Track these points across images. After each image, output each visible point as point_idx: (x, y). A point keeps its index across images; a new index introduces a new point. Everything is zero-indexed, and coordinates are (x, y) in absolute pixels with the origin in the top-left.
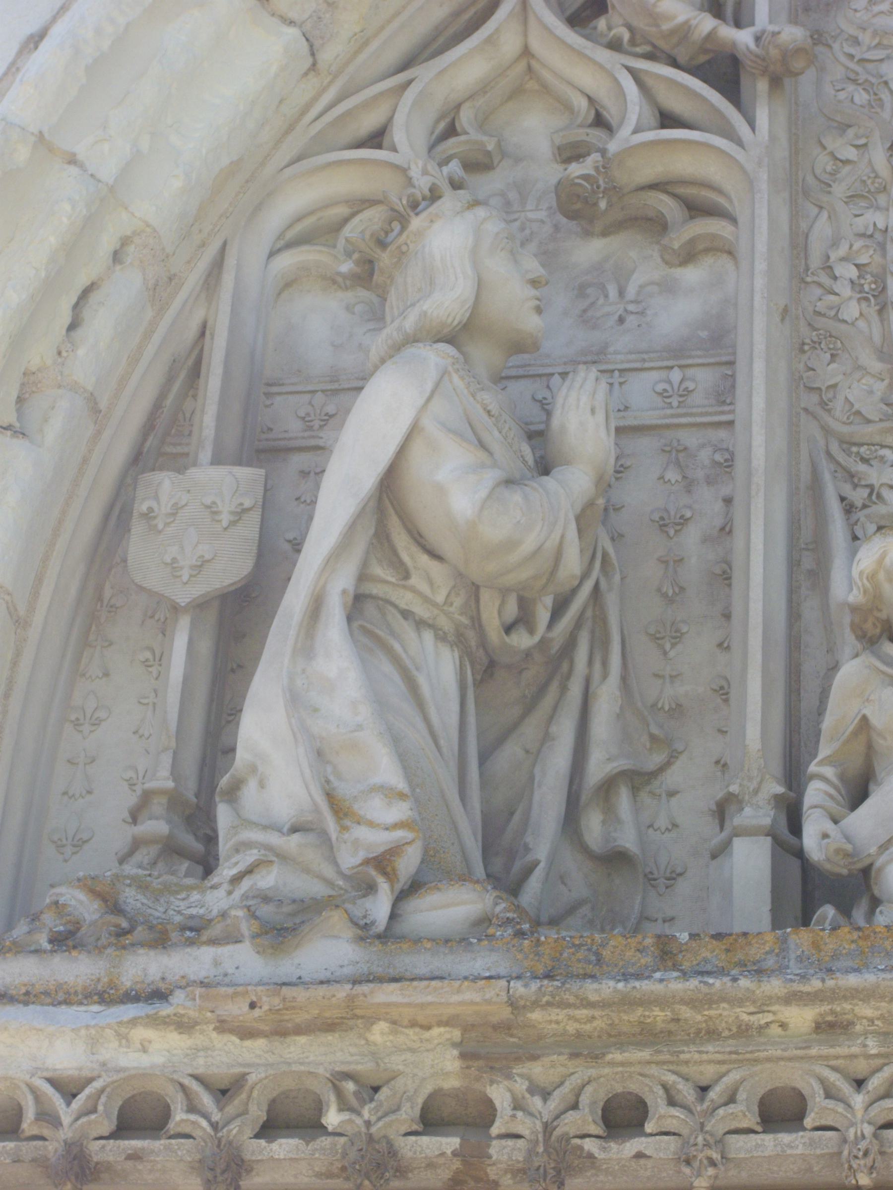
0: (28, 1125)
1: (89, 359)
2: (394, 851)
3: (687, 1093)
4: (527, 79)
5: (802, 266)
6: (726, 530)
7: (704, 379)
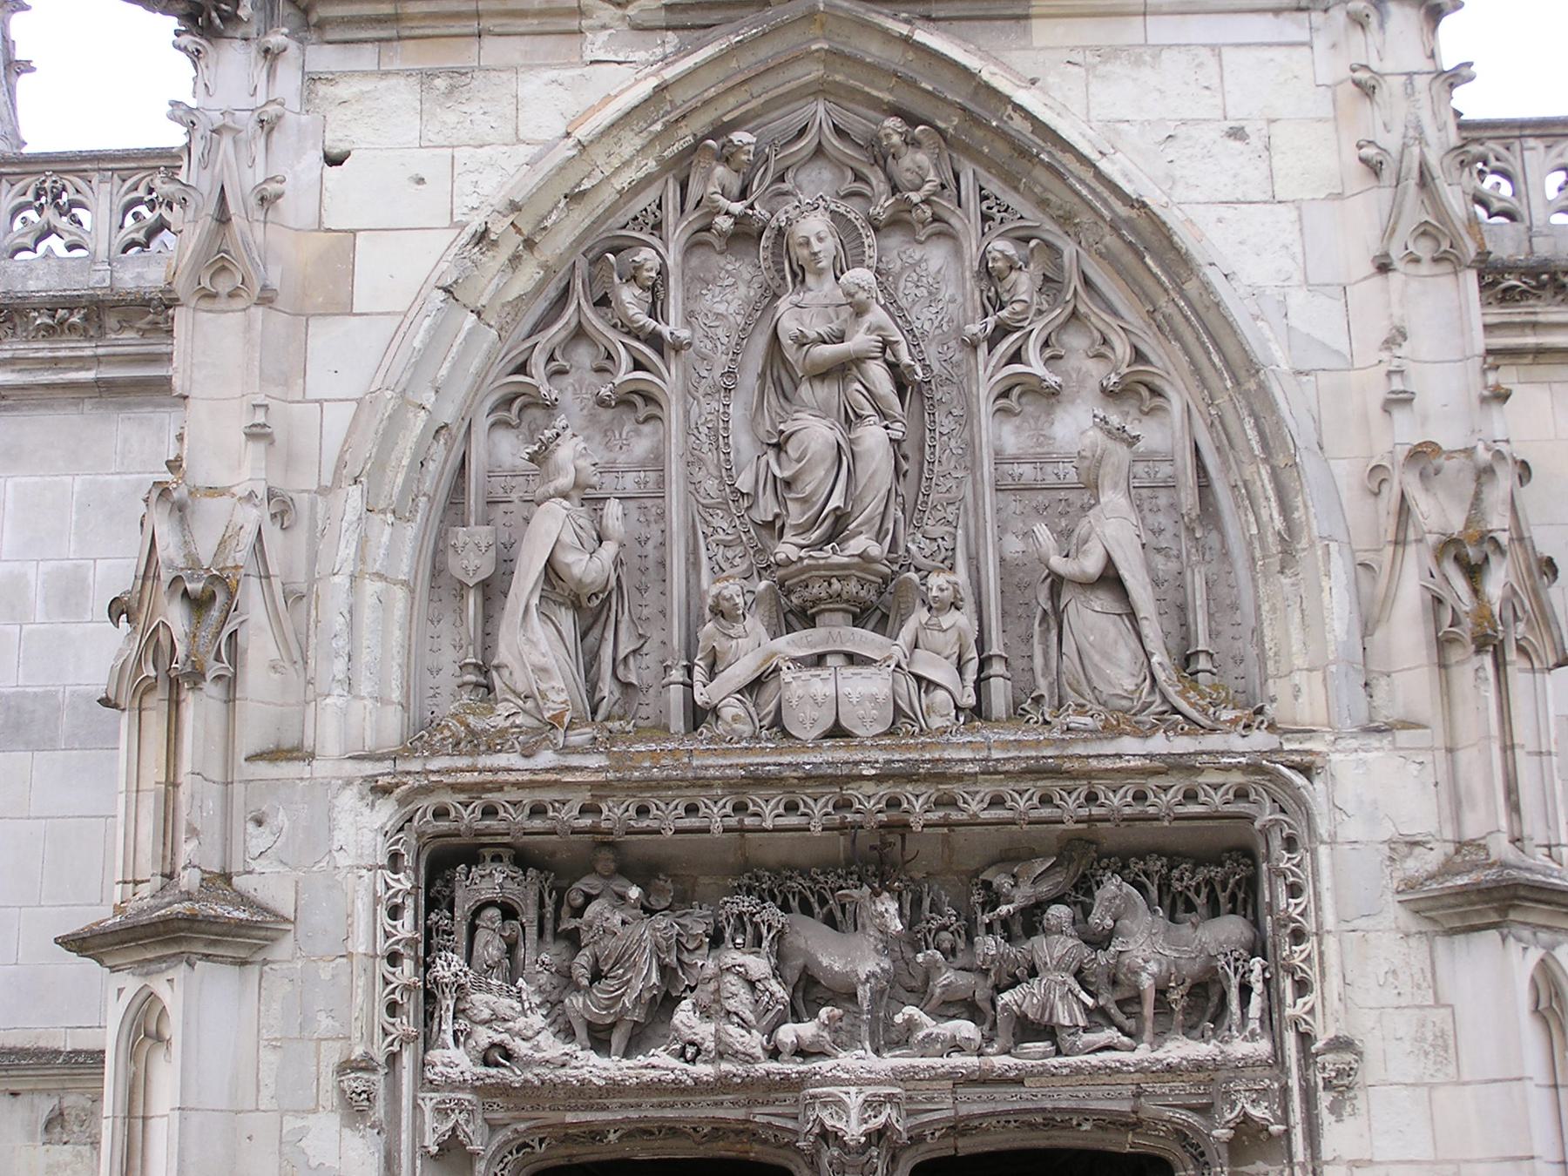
0: (453, 813)
1: (427, 486)
3: (662, 806)
4: (580, 333)
5: (689, 431)
6: (663, 544)
7: (652, 476)
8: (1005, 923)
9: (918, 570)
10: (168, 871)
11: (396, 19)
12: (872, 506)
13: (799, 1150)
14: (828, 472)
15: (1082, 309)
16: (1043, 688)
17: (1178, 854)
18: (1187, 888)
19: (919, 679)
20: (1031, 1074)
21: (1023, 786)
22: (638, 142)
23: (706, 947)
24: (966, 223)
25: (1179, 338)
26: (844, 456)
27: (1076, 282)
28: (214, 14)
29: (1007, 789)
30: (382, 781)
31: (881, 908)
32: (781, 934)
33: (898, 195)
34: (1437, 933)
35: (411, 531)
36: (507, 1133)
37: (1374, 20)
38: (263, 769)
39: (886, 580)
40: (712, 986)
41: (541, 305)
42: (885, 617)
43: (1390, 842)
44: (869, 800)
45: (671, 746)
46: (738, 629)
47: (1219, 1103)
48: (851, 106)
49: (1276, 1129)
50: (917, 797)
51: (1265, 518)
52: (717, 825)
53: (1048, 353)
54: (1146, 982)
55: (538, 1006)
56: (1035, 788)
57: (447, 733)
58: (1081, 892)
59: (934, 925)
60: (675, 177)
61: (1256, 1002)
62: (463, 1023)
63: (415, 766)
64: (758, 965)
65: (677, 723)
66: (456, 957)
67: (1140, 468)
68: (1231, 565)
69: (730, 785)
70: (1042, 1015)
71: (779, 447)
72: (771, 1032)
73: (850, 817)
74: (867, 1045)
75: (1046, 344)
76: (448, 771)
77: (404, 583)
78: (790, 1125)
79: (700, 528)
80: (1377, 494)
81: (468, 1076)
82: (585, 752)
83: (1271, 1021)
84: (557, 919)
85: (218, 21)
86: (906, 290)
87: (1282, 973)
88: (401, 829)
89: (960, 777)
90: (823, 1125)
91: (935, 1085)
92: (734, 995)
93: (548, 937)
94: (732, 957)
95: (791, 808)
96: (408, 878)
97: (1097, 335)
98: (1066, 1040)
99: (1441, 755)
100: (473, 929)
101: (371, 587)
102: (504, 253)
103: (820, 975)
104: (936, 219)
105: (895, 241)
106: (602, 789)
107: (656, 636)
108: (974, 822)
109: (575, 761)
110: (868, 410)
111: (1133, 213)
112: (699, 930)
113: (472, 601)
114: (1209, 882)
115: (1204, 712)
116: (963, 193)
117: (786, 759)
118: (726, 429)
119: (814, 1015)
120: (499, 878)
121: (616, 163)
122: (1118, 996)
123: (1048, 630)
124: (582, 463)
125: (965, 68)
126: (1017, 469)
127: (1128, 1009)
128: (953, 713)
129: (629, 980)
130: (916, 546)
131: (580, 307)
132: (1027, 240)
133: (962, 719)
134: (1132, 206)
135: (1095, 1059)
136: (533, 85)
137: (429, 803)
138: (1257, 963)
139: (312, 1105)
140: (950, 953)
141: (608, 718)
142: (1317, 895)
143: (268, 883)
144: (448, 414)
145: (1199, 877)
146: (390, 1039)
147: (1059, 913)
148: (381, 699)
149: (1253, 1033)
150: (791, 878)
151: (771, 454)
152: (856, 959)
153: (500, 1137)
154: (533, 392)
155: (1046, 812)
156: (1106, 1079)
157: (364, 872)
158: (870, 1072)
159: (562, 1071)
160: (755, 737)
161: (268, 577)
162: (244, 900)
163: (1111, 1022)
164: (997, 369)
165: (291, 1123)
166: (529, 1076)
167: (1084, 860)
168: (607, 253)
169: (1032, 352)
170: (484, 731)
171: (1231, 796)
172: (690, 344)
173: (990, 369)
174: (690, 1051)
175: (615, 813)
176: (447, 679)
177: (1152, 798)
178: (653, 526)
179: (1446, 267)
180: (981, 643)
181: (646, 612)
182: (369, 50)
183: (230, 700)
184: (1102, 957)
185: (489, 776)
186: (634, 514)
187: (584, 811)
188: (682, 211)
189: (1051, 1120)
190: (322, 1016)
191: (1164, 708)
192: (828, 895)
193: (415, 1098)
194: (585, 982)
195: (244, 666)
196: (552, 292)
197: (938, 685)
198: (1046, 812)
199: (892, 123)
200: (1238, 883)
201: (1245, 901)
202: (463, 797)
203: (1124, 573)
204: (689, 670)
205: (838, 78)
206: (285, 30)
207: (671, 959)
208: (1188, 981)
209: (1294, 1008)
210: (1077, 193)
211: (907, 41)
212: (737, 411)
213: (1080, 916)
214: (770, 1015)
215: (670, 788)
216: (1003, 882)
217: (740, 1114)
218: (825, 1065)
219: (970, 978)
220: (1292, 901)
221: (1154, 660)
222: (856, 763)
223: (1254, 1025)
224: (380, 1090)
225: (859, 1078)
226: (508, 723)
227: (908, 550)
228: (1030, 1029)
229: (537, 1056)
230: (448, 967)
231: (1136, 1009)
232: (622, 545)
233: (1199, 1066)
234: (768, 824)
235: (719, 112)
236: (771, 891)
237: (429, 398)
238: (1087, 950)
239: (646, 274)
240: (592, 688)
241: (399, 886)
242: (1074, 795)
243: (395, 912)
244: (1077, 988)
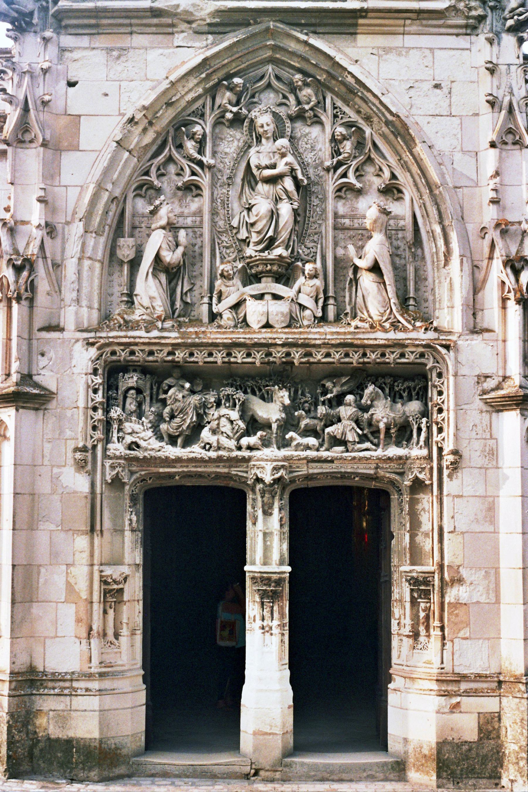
0: (118, 354)
1: (109, 221)
2: (161, 316)
5: (213, 200)
6: (202, 247)
7: (198, 219)
8: (330, 400)
9: (302, 260)
10: (7, 373)
11: (97, 26)
12: (284, 235)
13: (248, 485)
14: (267, 221)
15: (372, 156)
16: (348, 309)
17: (398, 376)
18: (400, 389)
19: (300, 305)
20: (337, 459)
21: (338, 350)
22: (195, 81)
23: (214, 408)
24: (326, 118)
25: (409, 171)
26: (274, 215)
27: (370, 145)
28: (22, 22)
29: (332, 351)
30: (91, 340)
33: (300, 106)
34: (493, 411)
35: (102, 240)
36: (138, 475)
37: (496, 41)
38: (45, 335)
39: (289, 264)
40: (216, 422)
41: (154, 148)
42: (288, 279)
43: (478, 376)
44: (278, 354)
45: (203, 329)
46: (231, 283)
47: (407, 472)
48: (282, 67)
49: (428, 482)
50: (297, 352)
51: (439, 246)
52: (219, 361)
53: (358, 174)
54: (382, 426)
55: (150, 428)
56: (342, 350)
57: (116, 322)
58: (358, 390)
59: (302, 401)
60: (210, 95)
61: (423, 435)
62: (121, 434)
63: (103, 335)
64: (235, 415)
65: (206, 319)
66: (119, 409)
67: (392, 222)
68: (425, 262)
69: (225, 345)
71: (249, 209)
72: (238, 440)
73: (271, 359)
74: (275, 446)
75: (357, 170)
76: (116, 337)
77: (99, 261)
78: (245, 475)
79: (217, 240)
80: (483, 238)
81: (123, 454)
82: (170, 331)
83: (428, 443)
84: (158, 394)
85: (24, 25)
86: (302, 145)
87: (434, 424)
88: (98, 359)
89: (314, 346)
90: (257, 476)
91: (301, 462)
93: (154, 402)
94: (223, 411)
95: (249, 355)
96: (100, 378)
97: (377, 167)
99: (500, 343)
100: (125, 398)
101: (87, 263)
102: (140, 128)
103: (258, 419)
104: (315, 116)
105: (298, 125)
106: (176, 346)
107: (198, 283)
108: (319, 362)
109: (165, 334)
110: (284, 197)
111: (394, 119)
112: (212, 400)
113: (126, 268)
114: (409, 388)
115: (409, 322)
116: (327, 106)
117: (247, 336)
118: (228, 200)
119: (255, 434)
120: (135, 378)
121: (186, 89)
122: (371, 430)
123: (352, 286)
124: (171, 215)
125: (329, 56)
126: (343, 221)
127: (376, 435)
128: (313, 319)
129: (185, 419)
130: (302, 251)
131: (170, 149)
132: (352, 126)
133: (316, 322)
134: (394, 116)
135: (362, 454)
136: (153, 55)
137: (108, 349)
138: (424, 420)
139: (64, 464)
140: (308, 412)
141: (179, 316)
142: (448, 395)
143: (47, 379)
144: (117, 192)
145: (405, 386)
146: (93, 440)
147: (350, 398)
148: (90, 307)
149: (421, 447)
150: (248, 381)
151: (245, 213)
153: (134, 477)
154: (151, 183)
155: (347, 360)
156: (365, 462)
157: (84, 376)
159: (158, 453)
160: (235, 326)
161: (46, 258)
162: (37, 385)
163: (368, 440)
164: (337, 180)
165: (55, 470)
166: (146, 454)
167: (360, 377)
168: (181, 125)
169: (351, 173)
170: (130, 321)
171: (418, 356)
172: (214, 166)
173: (334, 180)
174: (208, 447)
175: (180, 355)
176: (116, 298)
177: (387, 356)
178: (198, 239)
179: (517, 147)
180: (325, 291)
181: (194, 274)
182: (86, 38)
183: (31, 307)
184: (366, 416)
185: (132, 340)
186: (191, 234)
187: (169, 354)
188: (213, 109)
189: (344, 476)
190: (67, 430)
191: (395, 320)
192: (262, 388)
193: (102, 462)
194: (168, 419)
195: (37, 293)
196: (159, 142)
197: (307, 308)
199: (298, 76)
200: (420, 388)
201: (422, 395)
202: (122, 348)
203: (382, 266)
204: (211, 298)
205: (278, 56)
206: (51, 30)
207: (201, 411)
209: (436, 437)
210: (372, 109)
211: (306, 43)
212: (234, 193)
213: (358, 399)
214: (238, 434)
215: (202, 346)
216: (329, 385)
217: (226, 470)
219: (316, 421)
220: (439, 397)
221: (392, 301)
222: (275, 339)
223: (422, 443)
224: (90, 459)
226: (140, 318)
227: (298, 252)
228: (338, 441)
229: (149, 447)
230: (116, 412)
232: (186, 247)
233: (400, 458)
234: (239, 361)
235: (229, 69)
236: (240, 386)
237: (109, 187)
238: (360, 413)
239: (197, 136)
240: (173, 303)
241: (96, 381)
242: (358, 354)
243: (95, 391)
244: (356, 427)
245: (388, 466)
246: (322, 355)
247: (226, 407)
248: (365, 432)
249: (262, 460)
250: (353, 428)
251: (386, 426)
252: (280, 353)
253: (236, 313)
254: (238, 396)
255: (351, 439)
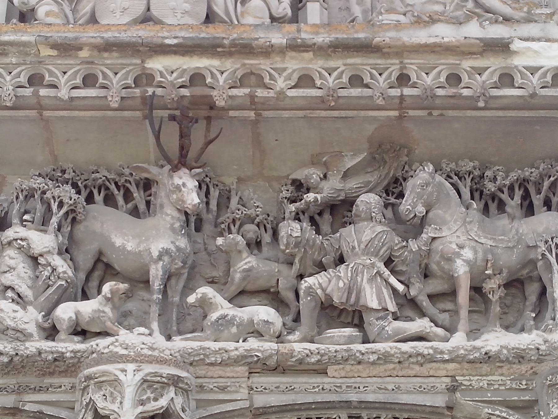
20: (335, 361)
21: (332, 64)
31: (177, 181)
32: (72, 217)
54: (461, 269)
70: (348, 299)
74: (155, 326)
91: (229, 371)
92: (12, 269)
95: (89, 81)
98: (373, 324)
114: (523, 183)
127: (442, 306)
145: (513, 176)
152: (149, 240)
158: (151, 348)
163: (423, 314)
177: (465, 78)
184: (413, 245)
192: (133, 188)
198: (356, 92)
208: (505, 271)
218: (102, 343)
219: (275, 267)
225: (139, 355)
231: (449, 306)
233: (520, 356)
234: (64, 93)
244: (387, 272)
245: (484, 384)
246: (289, 78)
247: (22, 222)
248: (413, 292)
249: (115, 358)
250: (378, 273)
251: (471, 272)
252: (175, 75)
253: (74, 11)
254: (57, 192)
255: (374, 304)
